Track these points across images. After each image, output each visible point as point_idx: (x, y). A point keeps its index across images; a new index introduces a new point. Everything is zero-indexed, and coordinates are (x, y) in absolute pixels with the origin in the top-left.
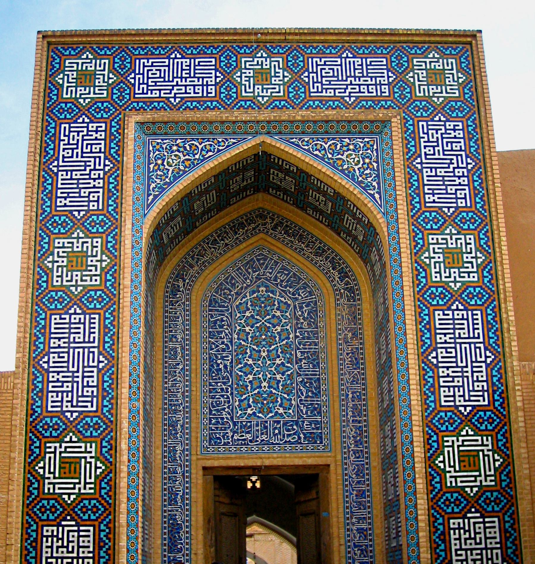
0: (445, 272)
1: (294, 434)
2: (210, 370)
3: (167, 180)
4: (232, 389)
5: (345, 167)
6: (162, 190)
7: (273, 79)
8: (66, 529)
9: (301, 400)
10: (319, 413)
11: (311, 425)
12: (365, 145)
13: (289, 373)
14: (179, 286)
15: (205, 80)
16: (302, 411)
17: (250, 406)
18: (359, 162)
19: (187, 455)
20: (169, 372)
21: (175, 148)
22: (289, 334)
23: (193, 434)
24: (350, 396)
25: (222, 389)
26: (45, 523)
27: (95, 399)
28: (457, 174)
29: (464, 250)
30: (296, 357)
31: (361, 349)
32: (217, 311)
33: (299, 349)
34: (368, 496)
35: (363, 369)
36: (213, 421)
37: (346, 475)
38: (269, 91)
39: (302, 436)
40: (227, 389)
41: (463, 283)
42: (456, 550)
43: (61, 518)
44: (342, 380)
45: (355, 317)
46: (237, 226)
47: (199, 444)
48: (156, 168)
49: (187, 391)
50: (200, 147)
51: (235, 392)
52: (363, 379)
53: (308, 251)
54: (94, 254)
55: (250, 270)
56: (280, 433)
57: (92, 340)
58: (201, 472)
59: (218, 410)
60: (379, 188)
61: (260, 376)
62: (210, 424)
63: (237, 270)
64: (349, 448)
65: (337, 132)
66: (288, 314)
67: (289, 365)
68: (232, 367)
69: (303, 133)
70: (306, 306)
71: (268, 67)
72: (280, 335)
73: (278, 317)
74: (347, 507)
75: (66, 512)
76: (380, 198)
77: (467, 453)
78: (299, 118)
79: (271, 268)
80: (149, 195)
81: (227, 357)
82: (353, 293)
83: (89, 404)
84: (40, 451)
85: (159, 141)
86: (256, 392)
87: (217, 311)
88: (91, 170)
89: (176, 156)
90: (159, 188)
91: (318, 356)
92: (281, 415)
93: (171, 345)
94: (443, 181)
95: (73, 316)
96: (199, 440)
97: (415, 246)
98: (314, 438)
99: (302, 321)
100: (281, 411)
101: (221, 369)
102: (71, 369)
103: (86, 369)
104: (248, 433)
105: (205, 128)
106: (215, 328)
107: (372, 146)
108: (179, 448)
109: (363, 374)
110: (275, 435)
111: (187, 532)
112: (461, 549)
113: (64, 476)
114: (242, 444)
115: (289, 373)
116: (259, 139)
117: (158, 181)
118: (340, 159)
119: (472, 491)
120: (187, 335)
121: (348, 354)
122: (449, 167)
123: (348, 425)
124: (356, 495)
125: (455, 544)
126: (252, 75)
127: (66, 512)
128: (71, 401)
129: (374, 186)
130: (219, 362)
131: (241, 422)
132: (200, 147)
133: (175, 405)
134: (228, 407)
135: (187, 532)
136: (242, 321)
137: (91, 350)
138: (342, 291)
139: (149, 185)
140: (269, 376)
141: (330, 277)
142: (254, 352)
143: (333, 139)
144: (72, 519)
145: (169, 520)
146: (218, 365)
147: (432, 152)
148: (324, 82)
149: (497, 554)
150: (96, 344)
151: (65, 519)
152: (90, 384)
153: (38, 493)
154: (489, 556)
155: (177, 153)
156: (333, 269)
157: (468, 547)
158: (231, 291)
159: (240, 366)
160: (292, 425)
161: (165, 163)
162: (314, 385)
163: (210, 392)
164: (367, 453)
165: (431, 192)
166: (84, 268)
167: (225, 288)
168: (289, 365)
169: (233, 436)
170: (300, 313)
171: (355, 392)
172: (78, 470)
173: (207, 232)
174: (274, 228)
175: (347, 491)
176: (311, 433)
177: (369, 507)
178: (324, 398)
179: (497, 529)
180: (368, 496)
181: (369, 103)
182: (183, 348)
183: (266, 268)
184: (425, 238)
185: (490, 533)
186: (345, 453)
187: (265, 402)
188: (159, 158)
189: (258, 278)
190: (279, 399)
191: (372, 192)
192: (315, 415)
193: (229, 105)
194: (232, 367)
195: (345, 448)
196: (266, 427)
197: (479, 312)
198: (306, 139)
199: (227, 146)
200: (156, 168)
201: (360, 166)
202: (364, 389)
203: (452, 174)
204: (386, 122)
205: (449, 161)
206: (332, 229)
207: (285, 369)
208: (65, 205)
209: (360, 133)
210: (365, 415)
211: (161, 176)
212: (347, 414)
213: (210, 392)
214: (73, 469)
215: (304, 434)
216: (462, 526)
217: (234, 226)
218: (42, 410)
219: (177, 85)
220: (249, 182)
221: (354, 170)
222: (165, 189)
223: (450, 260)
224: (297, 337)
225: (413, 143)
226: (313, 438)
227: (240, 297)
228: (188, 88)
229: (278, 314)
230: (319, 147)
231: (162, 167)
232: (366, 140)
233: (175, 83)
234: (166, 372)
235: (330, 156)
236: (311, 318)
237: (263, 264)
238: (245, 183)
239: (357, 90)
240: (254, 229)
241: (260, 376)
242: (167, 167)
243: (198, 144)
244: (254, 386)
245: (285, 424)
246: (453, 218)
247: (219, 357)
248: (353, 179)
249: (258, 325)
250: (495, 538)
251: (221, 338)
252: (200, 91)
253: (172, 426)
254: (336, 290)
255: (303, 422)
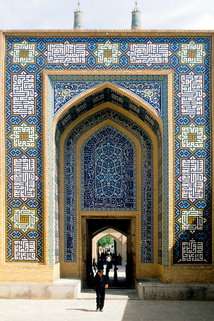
0: (188, 143)
1: (121, 204)
2: (85, 177)
3: (63, 101)
4: (94, 185)
5: (145, 96)
6: (61, 105)
7: (113, 54)
8: (24, 242)
9: (124, 190)
10: (132, 196)
11: (128, 200)
12: (155, 86)
13: (120, 179)
14: (70, 142)
15: (81, 55)
16: (125, 194)
17: (102, 192)
18: (151, 94)
19: (75, 211)
20: (67, 177)
21: (66, 87)
22: (120, 163)
23: (77, 203)
24: (146, 189)
25: (90, 185)
26: (15, 239)
27: (34, 193)
28: (197, 100)
29: (198, 134)
30: (123, 172)
31: (152, 170)
32: (88, 152)
33: (124, 169)
34: (152, 229)
35: (152, 178)
36: (86, 198)
37: (143, 220)
38: (111, 60)
39: (124, 204)
40: (92, 185)
41: (196, 148)
42: (184, 254)
43: (21, 238)
44: (143, 182)
45: (150, 156)
46: (97, 116)
47: (80, 207)
48: (58, 96)
49: (75, 186)
50: (78, 87)
51: (96, 186)
52: (152, 182)
53: (129, 127)
54: (31, 133)
55: (103, 135)
56: (115, 203)
57: (32, 169)
58: (81, 218)
59: (88, 194)
60: (160, 106)
61: (107, 180)
62: (85, 199)
63: (97, 135)
64: (145, 210)
65: (142, 80)
66: (120, 154)
67: (120, 176)
68: (94, 176)
69: (126, 80)
70: (128, 151)
71: (111, 49)
72: (116, 163)
73: (115, 156)
74: (143, 233)
75: (24, 236)
76: (161, 110)
77: (192, 217)
78: (124, 74)
79: (113, 134)
80: (55, 108)
81: (93, 172)
82: (149, 145)
83: (32, 195)
84: (12, 213)
85: (59, 83)
86: (105, 186)
87: (88, 152)
88: (28, 97)
89: (67, 90)
90: (60, 105)
91: (133, 172)
92: (116, 196)
93: (67, 167)
94: (191, 103)
95: (23, 160)
96: (80, 205)
97: (175, 132)
98: (130, 205)
99: (126, 157)
100: (116, 194)
101: (89, 177)
102: (23, 181)
103: (30, 181)
104: (101, 203)
105: (80, 78)
106: (87, 160)
107: (158, 86)
108: (71, 208)
109: (152, 180)
110: (112, 204)
111: (75, 241)
112: (186, 253)
113: (22, 222)
114: (98, 207)
115: (120, 179)
116: (105, 83)
117: (59, 102)
118: (143, 93)
119: (192, 232)
120: (75, 162)
121: (146, 172)
122: (194, 97)
123: (144, 201)
124: (147, 228)
125: (184, 252)
126: (103, 52)
127: (24, 236)
128: (24, 194)
129: (158, 105)
130: (89, 174)
131: (98, 198)
132: (78, 87)
133: (69, 191)
134: (93, 192)
135: (75, 241)
136: (99, 157)
137: (32, 173)
138: (145, 145)
139: (55, 104)
140: (111, 180)
141: (139, 139)
142: (104, 170)
143: (140, 83)
144: (26, 238)
145: (67, 236)
146: (88, 175)
147: (186, 90)
148: (137, 56)
149: (201, 256)
150: (34, 171)
151: (23, 238)
152: (32, 187)
153: (12, 228)
154: (198, 256)
155: (67, 89)
156: (141, 135)
157: (189, 252)
158: (94, 144)
159: (98, 176)
160: (120, 200)
161: (62, 94)
162: (130, 185)
163: (85, 186)
164: (152, 212)
165: (184, 108)
166: (27, 139)
167: (92, 143)
168: (120, 176)
169: (94, 204)
170: (125, 154)
171: (149, 188)
172: (28, 220)
173: (83, 118)
174: (114, 117)
175: (143, 227)
176: (128, 203)
177: (152, 233)
178: (135, 189)
179: (202, 247)
180: (152, 229)
181: (158, 66)
182: (73, 168)
183: (110, 134)
184: (180, 129)
185: (199, 248)
186: (143, 212)
187: (109, 191)
188: (59, 91)
189: (107, 138)
190: (115, 190)
191: (157, 108)
192: (130, 196)
193: (91, 67)
194: (94, 176)
195: (143, 210)
196: (109, 201)
197: (202, 161)
198: (127, 83)
199: (91, 86)
200: (58, 96)
201: (152, 96)
202: (152, 186)
203: (195, 100)
204: (165, 77)
205: (194, 94)
206: (141, 119)
207: (118, 177)
208: (17, 112)
209: (153, 80)
210: (152, 197)
211: (60, 99)
212: (144, 196)
213: (85, 186)
214: (26, 220)
215: (125, 204)
216: (187, 245)
217: (96, 116)
218: (12, 197)
219: (67, 57)
220: (102, 98)
221: (149, 98)
222: (62, 106)
223: (191, 138)
224: (123, 164)
225: (178, 85)
226: (129, 205)
227: (98, 147)
228: (72, 58)
229: (115, 154)
230: (133, 87)
231: (60, 96)
232: (156, 84)
233: (66, 56)
234: (65, 178)
235: (138, 91)
236: (130, 156)
237: (109, 133)
238: (100, 99)
239: (153, 60)
240: (105, 117)
241: (107, 180)
242: (63, 95)
243: (77, 85)
244: (104, 184)
245: (117, 199)
246: (194, 120)
247: (89, 172)
248: (148, 102)
249: (106, 159)
250: (201, 250)
251: (90, 164)
252: (78, 60)
253: (68, 199)
254: (142, 144)
255: (125, 199)
